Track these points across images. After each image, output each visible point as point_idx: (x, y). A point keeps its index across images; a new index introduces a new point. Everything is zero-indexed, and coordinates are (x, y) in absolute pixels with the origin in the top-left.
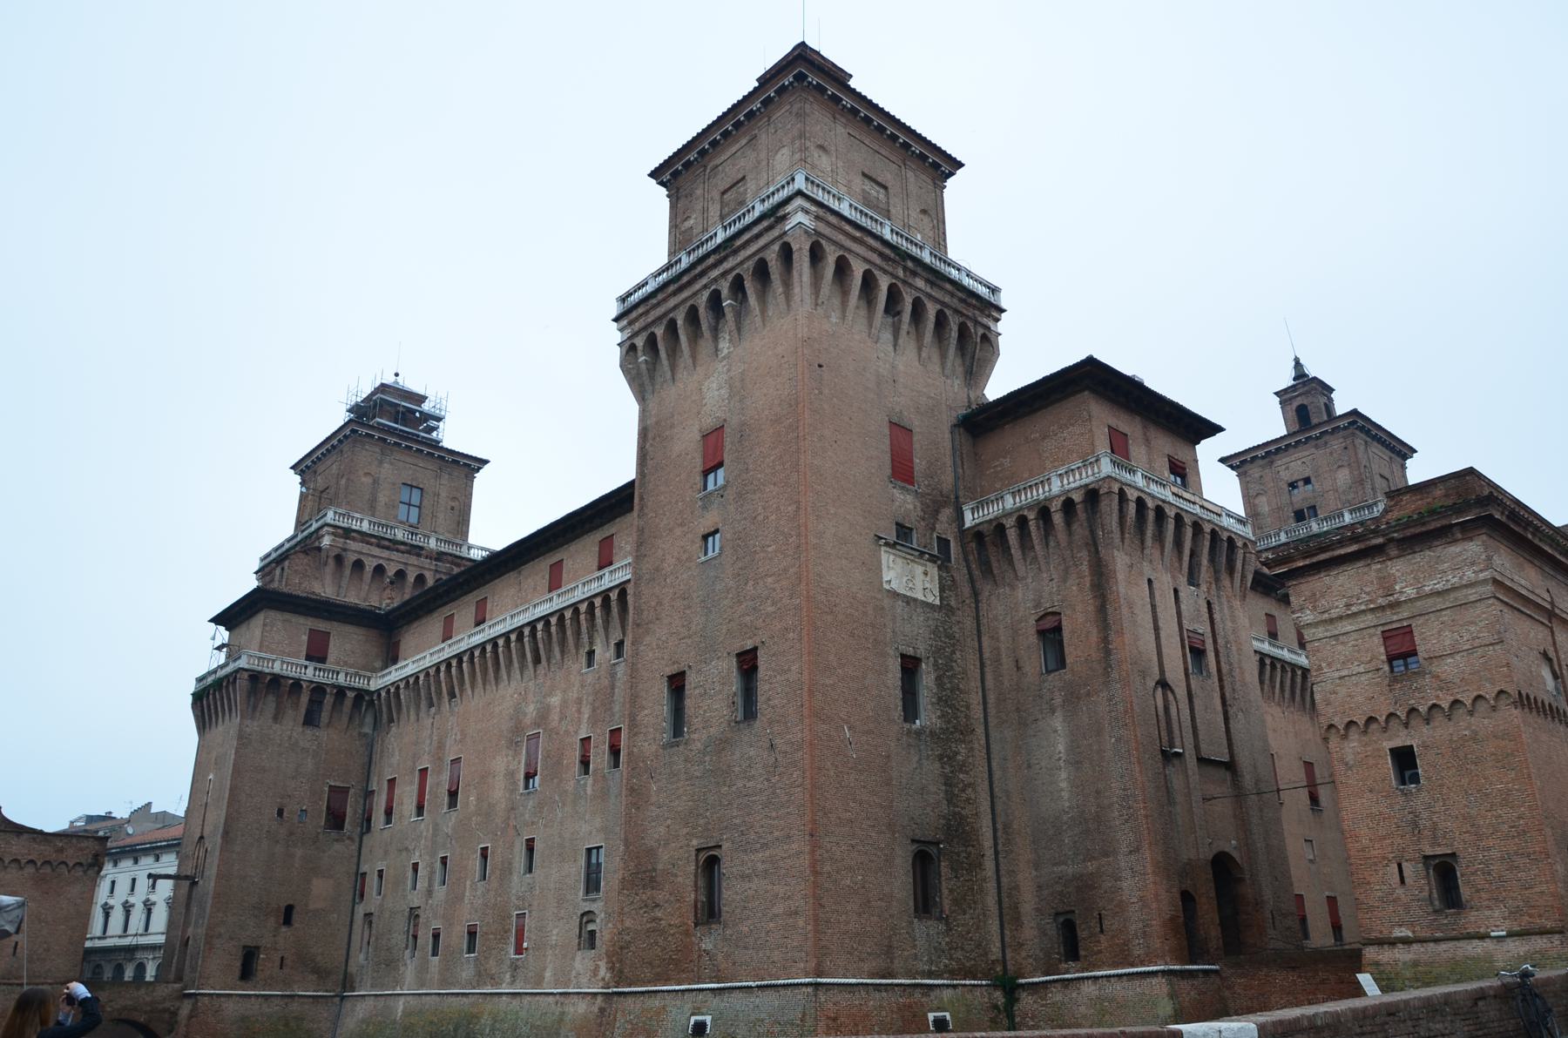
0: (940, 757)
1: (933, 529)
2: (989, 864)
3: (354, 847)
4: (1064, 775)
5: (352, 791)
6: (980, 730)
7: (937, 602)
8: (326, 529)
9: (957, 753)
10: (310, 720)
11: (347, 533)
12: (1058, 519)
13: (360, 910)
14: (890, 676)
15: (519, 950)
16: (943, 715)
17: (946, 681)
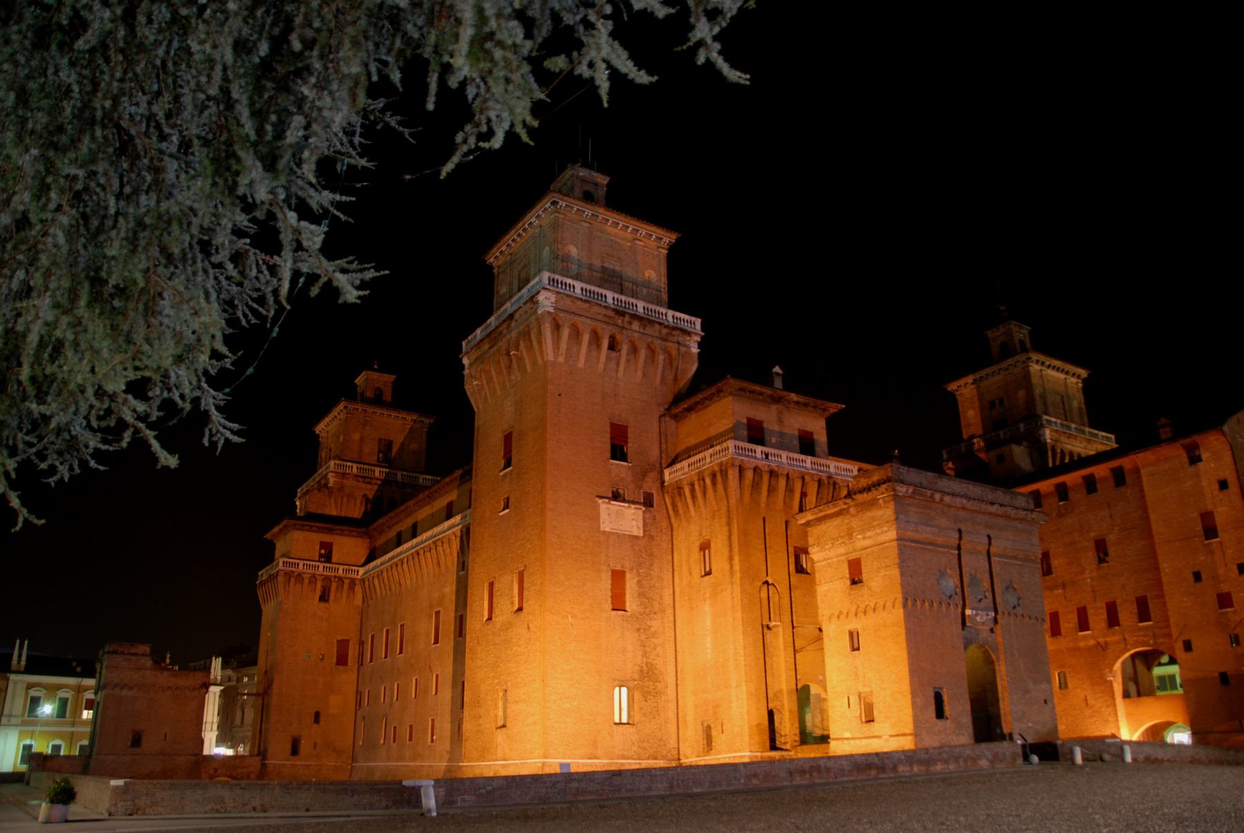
0: (638, 630)
1: (641, 487)
2: (671, 692)
3: (354, 676)
4: (709, 639)
5: (351, 642)
6: (669, 611)
7: (642, 535)
8: (330, 474)
9: (650, 627)
10: (324, 598)
11: (344, 475)
12: (708, 481)
13: (359, 713)
14: (603, 583)
15: (432, 741)
16: (641, 604)
17: (644, 582)
